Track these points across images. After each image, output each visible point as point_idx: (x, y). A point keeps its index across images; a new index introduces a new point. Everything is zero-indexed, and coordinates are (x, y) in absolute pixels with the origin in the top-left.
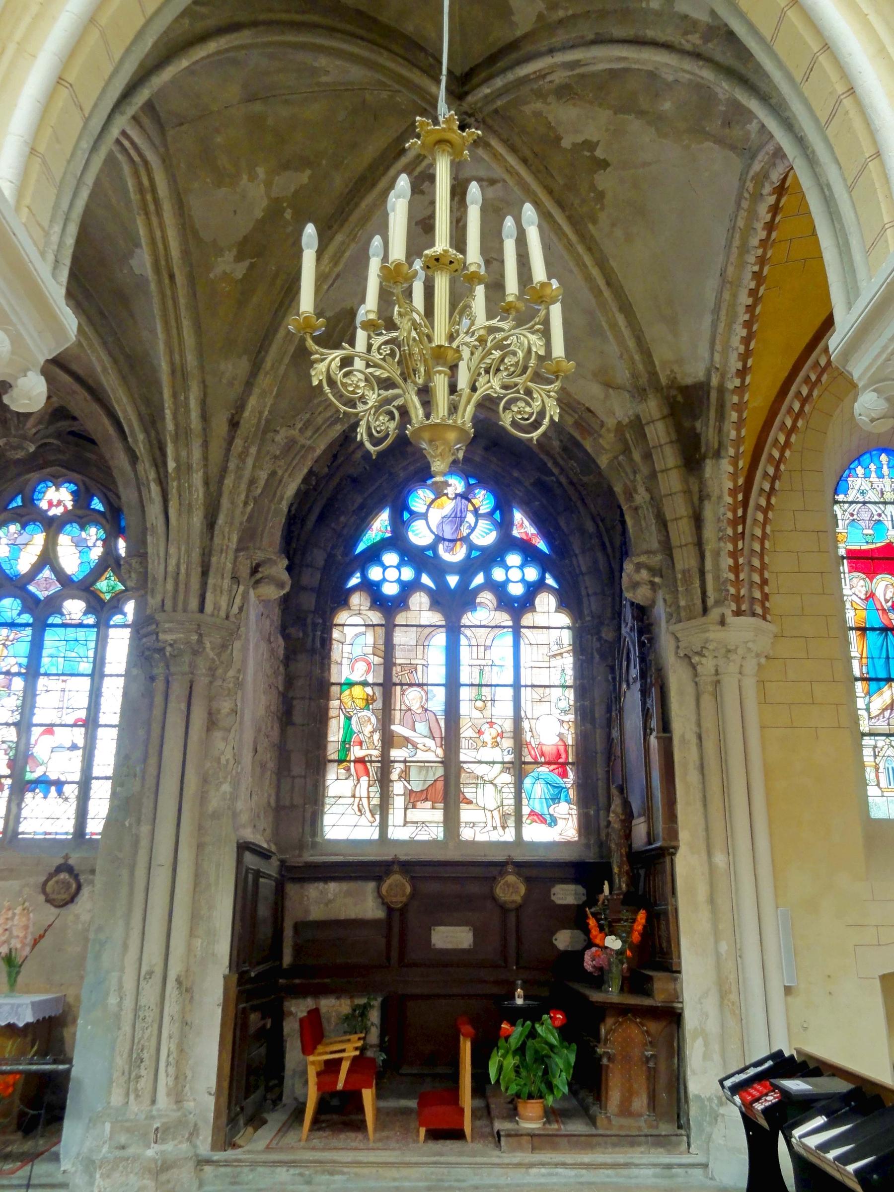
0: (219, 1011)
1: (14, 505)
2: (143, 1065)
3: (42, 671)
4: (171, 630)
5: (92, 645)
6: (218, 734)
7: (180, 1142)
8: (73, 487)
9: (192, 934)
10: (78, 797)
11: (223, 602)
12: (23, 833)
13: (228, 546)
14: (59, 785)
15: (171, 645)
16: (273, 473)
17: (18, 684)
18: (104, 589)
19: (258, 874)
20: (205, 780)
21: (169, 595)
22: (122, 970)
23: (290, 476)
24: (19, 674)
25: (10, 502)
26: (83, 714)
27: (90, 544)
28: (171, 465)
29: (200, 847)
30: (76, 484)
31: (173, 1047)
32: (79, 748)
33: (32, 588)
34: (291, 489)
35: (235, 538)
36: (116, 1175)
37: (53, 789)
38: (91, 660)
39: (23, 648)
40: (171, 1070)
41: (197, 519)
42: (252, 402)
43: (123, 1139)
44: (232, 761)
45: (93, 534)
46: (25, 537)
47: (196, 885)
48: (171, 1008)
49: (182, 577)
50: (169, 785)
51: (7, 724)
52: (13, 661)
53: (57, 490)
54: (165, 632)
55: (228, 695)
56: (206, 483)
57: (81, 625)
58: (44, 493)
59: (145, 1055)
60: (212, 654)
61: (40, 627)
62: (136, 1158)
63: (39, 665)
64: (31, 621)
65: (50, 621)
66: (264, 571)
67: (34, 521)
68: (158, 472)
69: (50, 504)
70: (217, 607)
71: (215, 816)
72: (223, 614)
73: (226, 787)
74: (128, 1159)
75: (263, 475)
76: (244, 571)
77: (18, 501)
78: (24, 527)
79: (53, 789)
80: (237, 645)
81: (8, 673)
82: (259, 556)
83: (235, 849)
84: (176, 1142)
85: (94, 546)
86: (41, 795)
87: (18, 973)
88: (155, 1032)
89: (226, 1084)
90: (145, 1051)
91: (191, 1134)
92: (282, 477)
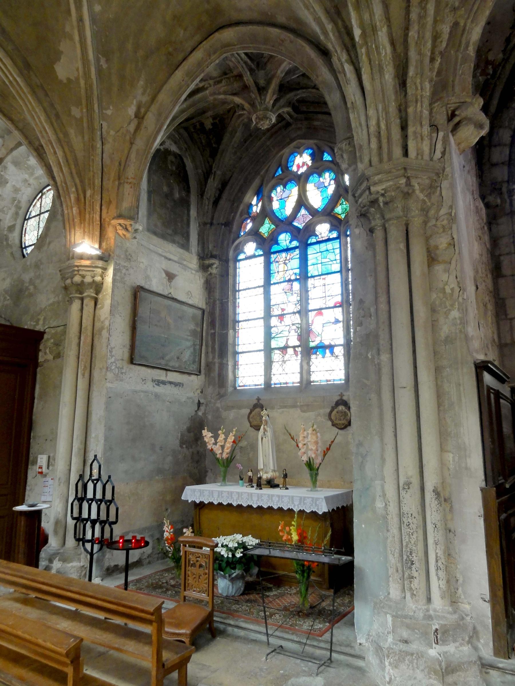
0: (481, 522)
1: (277, 174)
2: (414, 567)
3: (309, 275)
4: (380, 182)
5: (338, 251)
6: (439, 268)
7: (461, 645)
8: (310, 151)
9: (442, 449)
10: (344, 355)
11: (426, 148)
12: (313, 382)
13: (422, 96)
14: (331, 347)
15: (383, 195)
16: (456, 24)
17: (296, 286)
18: (340, 213)
19: (498, 395)
20: (433, 310)
21: (375, 152)
22: (383, 479)
23: (472, 22)
24: (296, 280)
25: (275, 173)
26: (339, 299)
27: (326, 184)
28: (357, 33)
29: (438, 370)
30: (311, 149)
31: (440, 553)
32: (340, 322)
33: (295, 224)
34: (476, 33)
35: (427, 85)
36: (403, 666)
37: (327, 351)
38: (339, 261)
39: (295, 263)
40: (441, 574)
41: (389, 76)
43: (405, 634)
44: (457, 289)
45: (328, 177)
46: (287, 192)
47: (439, 405)
48: (433, 516)
49: (383, 133)
50: (401, 316)
51: (294, 313)
52: (291, 272)
53: (301, 156)
54: (375, 184)
55: (444, 231)
56: (393, 43)
57: (329, 240)
58: (294, 161)
59: (415, 559)
60: (421, 196)
61: (304, 246)
62: (420, 655)
63: (306, 272)
64: (298, 245)
65: (309, 242)
66: (461, 114)
67: (290, 180)
68: (349, 54)
69: (298, 167)
70: (420, 153)
71: (448, 340)
72: (426, 157)
73: (455, 314)
74: (412, 654)
75: (445, 29)
76: (441, 119)
77: (280, 172)
78: (285, 187)
79: (327, 351)
80: (445, 184)
81: (290, 280)
82: (453, 101)
83: (474, 369)
84: (457, 644)
85: (329, 185)
86: (320, 356)
87: (317, 474)
88: (421, 538)
89: (500, 593)
90: (414, 555)
91: (471, 637)
92: (465, 25)
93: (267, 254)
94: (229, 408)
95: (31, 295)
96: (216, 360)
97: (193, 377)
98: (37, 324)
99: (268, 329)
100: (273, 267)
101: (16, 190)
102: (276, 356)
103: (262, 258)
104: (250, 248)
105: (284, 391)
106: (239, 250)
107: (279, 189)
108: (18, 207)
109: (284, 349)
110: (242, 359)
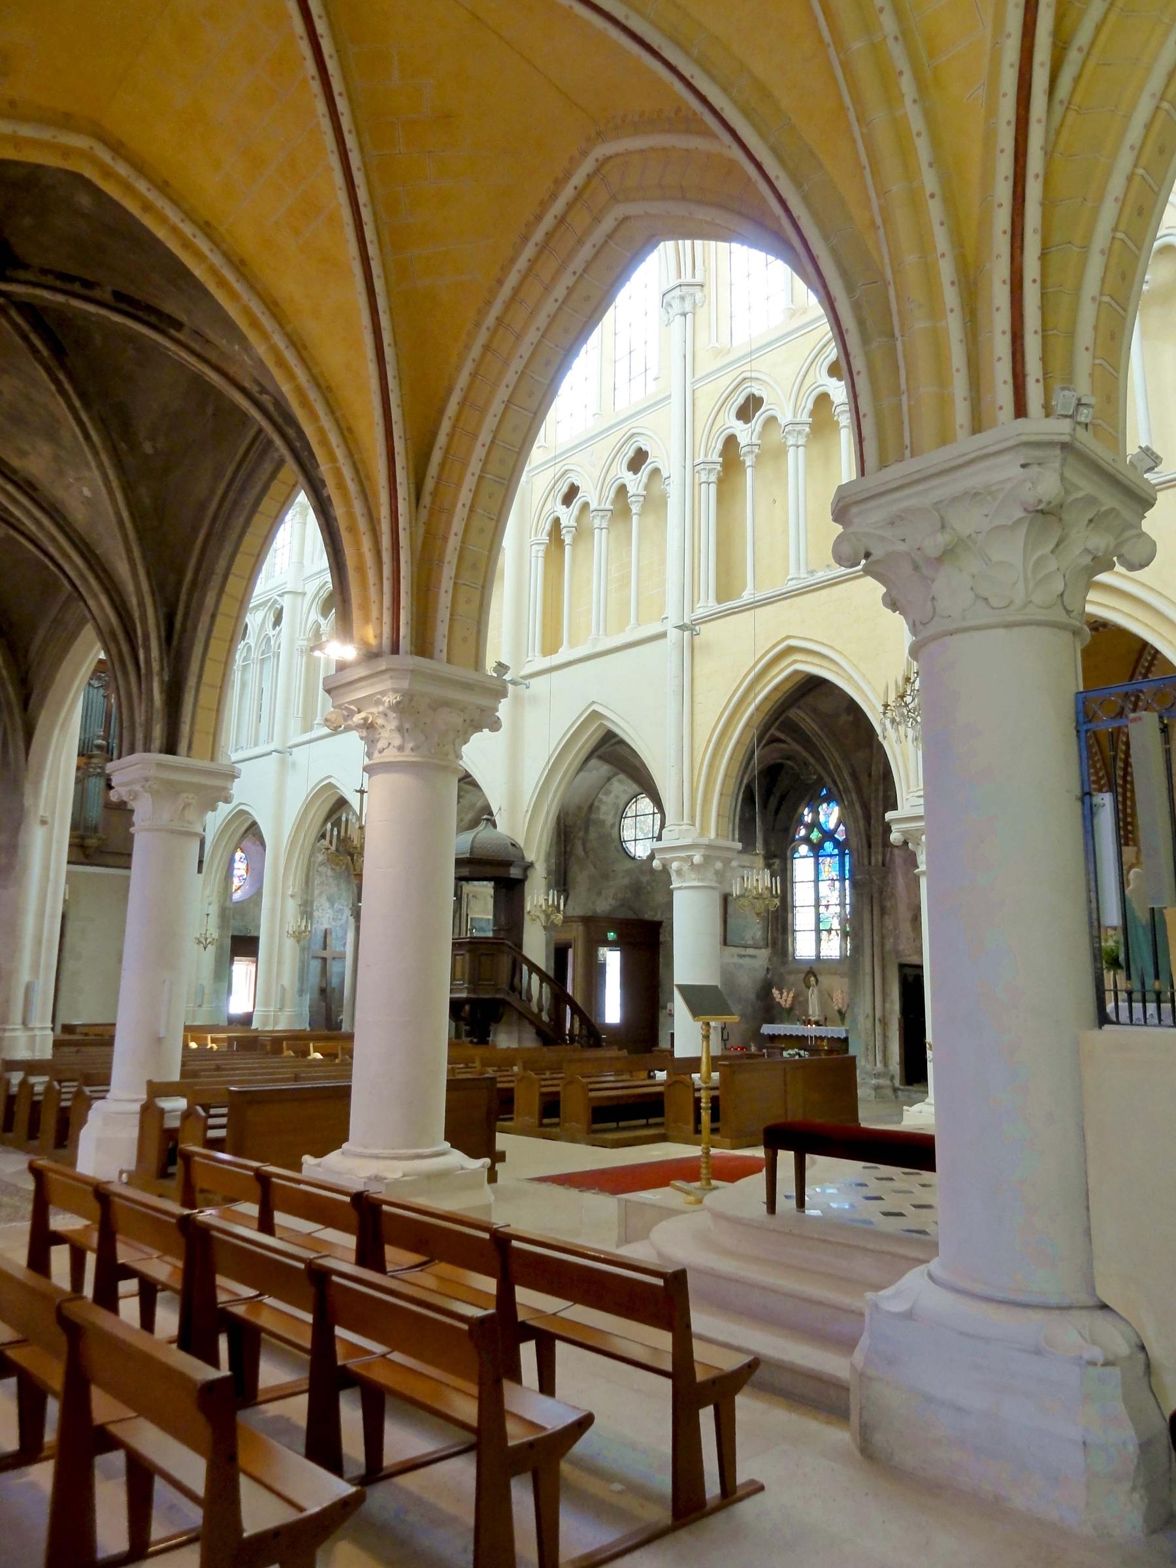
6: (887, 917)
17: (837, 884)
20: (883, 937)
41: (862, 823)
42: (874, 768)
70: (877, 861)
73: (892, 940)
77: (824, 792)
93: (817, 857)
94: (790, 973)
95: (649, 893)
96: (780, 936)
97: (763, 950)
98: (656, 913)
99: (818, 915)
100: (821, 866)
101: (617, 797)
102: (824, 935)
103: (812, 860)
104: (803, 849)
105: (830, 962)
106: (795, 850)
107: (825, 805)
108: (618, 808)
109: (829, 931)
110: (798, 935)
